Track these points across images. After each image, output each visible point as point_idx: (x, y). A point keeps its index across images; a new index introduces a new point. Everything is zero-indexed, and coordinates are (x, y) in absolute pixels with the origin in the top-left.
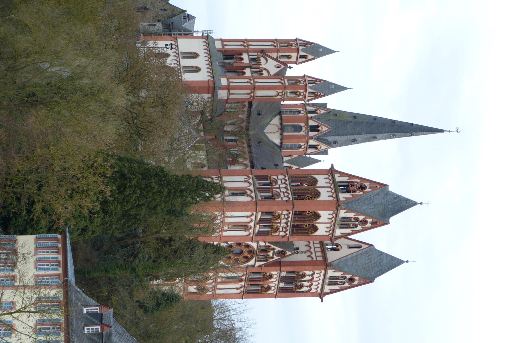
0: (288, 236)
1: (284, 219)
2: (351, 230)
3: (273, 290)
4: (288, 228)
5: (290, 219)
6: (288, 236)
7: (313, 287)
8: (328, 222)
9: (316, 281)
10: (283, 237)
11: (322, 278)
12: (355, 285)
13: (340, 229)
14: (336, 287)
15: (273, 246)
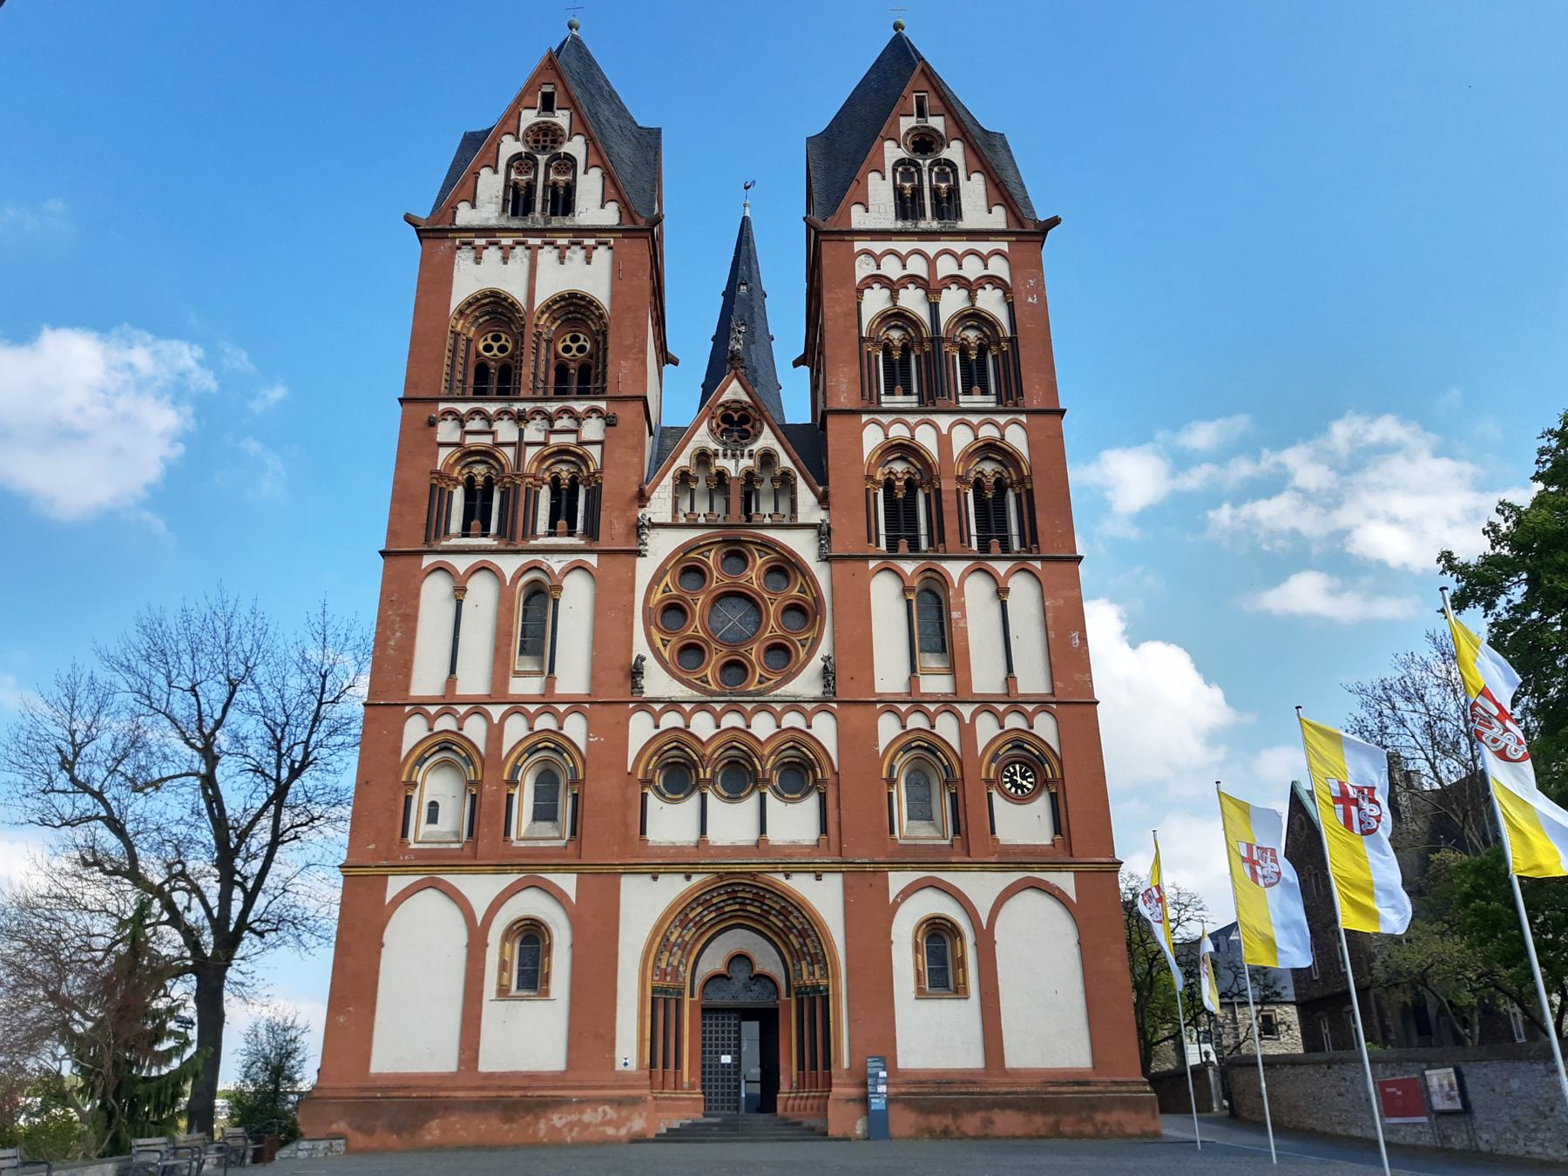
0: (603, 405)
1: (493, 433)
2: (586, 172)
3: (1001, 429)
4: (552, 407)
5: (492, 408)
6: (603, 405)
7: (972, 269)
8: (526, 261)
9: (931, 263)
10: (610, 422)
11: (904, 247)
12: (950, 122)
13: (577, 210)
14: (973, 190)
15: (684, 461)
